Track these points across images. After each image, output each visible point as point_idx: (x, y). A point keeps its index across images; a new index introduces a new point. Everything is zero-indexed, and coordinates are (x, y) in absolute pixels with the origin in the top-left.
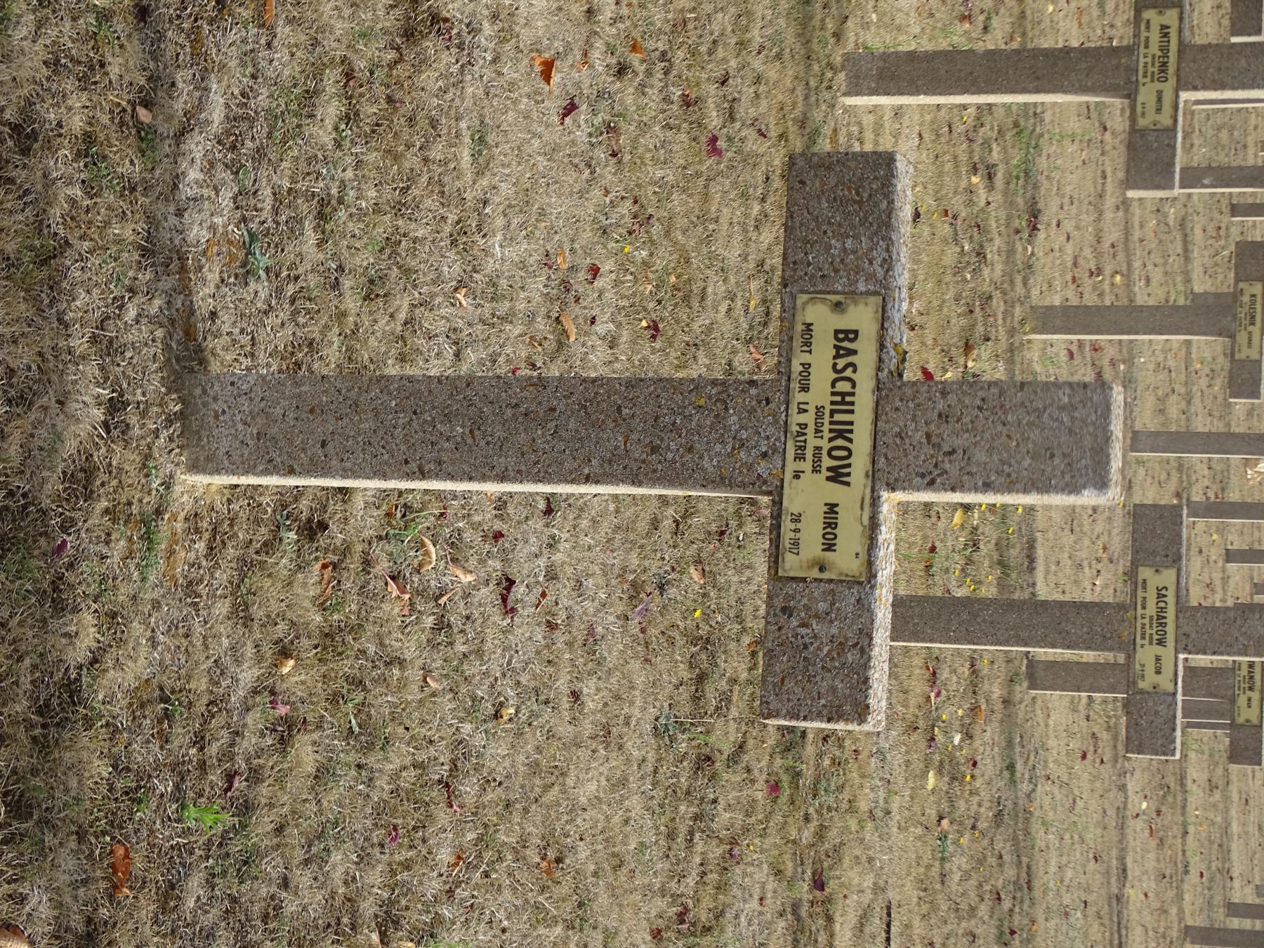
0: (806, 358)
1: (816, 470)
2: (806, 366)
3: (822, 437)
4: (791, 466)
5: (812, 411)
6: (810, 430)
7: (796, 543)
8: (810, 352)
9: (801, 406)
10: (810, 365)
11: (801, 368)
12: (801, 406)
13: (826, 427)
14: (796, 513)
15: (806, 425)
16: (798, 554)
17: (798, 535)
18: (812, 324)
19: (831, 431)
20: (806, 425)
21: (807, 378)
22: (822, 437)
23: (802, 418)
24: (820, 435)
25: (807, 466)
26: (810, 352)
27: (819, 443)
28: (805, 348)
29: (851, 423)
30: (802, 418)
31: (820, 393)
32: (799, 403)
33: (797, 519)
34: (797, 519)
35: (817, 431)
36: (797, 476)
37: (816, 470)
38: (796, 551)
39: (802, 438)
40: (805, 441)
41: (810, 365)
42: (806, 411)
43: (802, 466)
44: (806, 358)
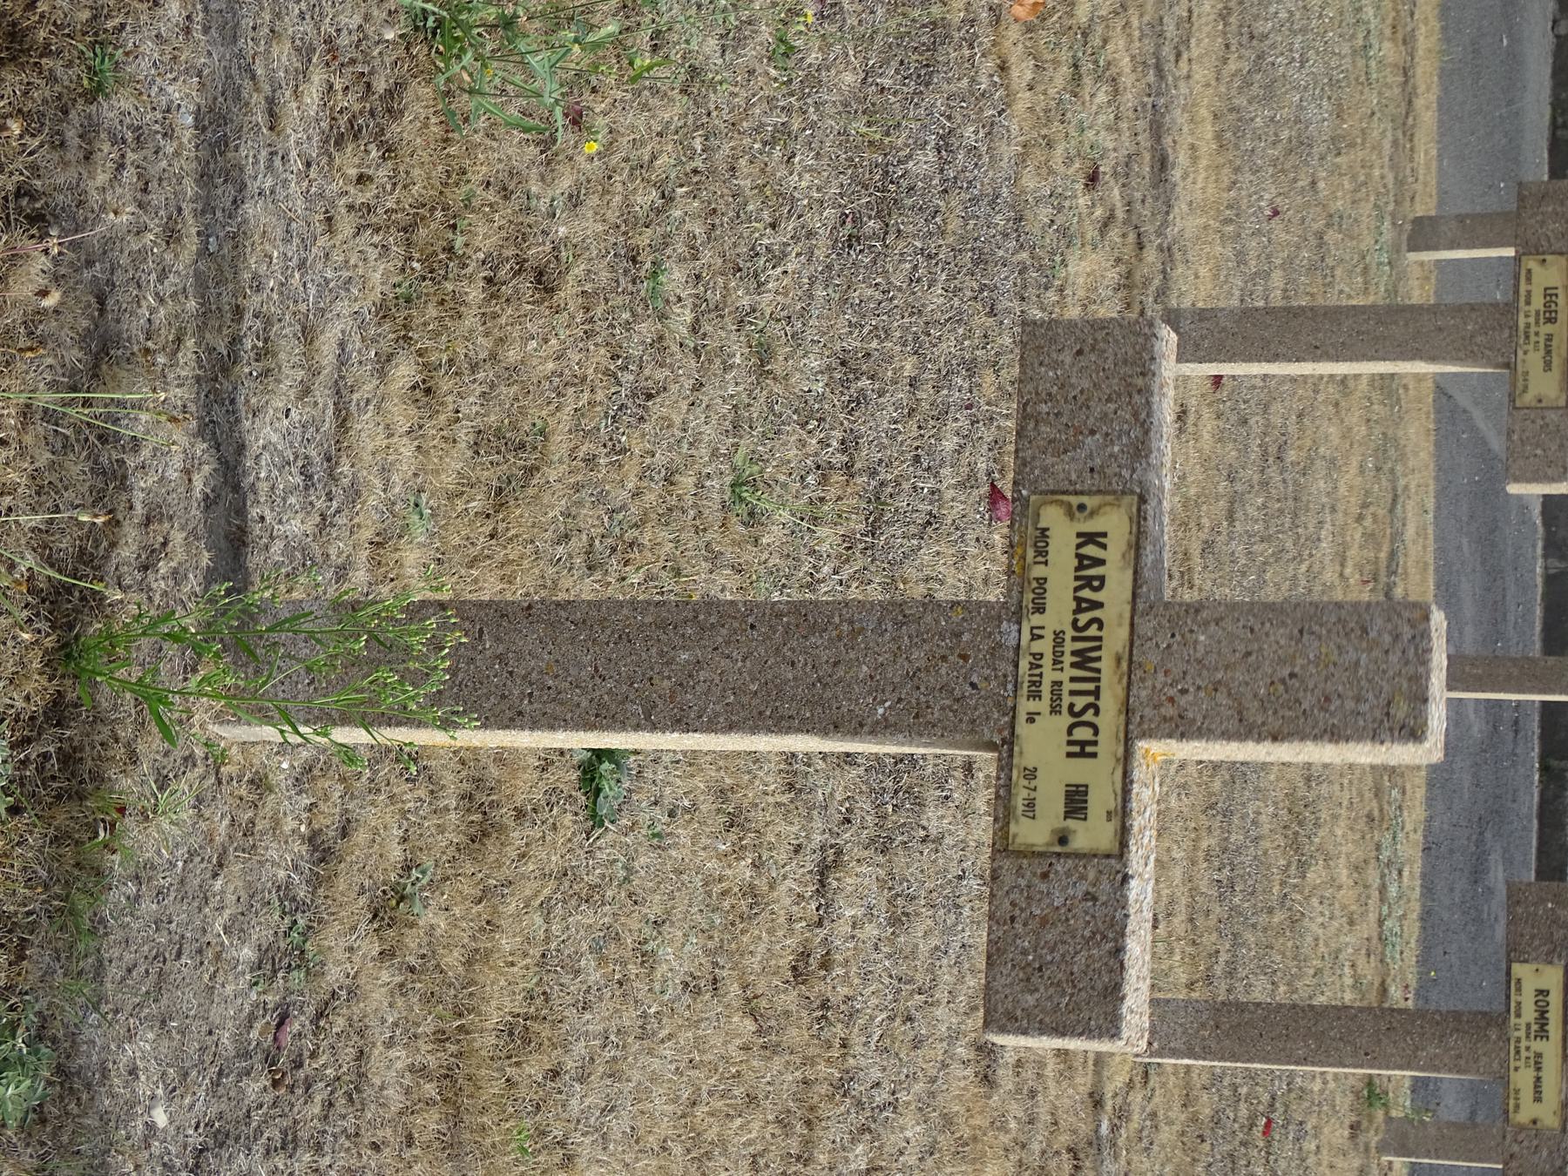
0: (1038, 571)
1: (1055, 710)
2: (1042, 581)
3: (1062, 669)
4: (1025, 706)
5: (1049, 637)
6: (1047, 661)
7: (1031, 805)
8: (1046, 563)
9: (1035, 631)
10: (1045, 579)
11: (1035, 584)
12: (1035, 631)
13: (1068, 659)
14: (1030, 767)
15: (1042, 655)
16: (1034, 818)
17: (1033, 795)
18: (1048, 529)
19: (1074, 653)
20: (1042, 655)
21: (1041, 596)
22: (1062, 669)
23: (1037, 647)
24: (1059, 666)
25: (1043, 705)
26: (1046, 563)
27: (1057, 676)
28: (1040, 559)
29: (1099, 639)
30: (1037, 647)
31: (1059, 612)
32: (1032, 628)
33: (1031, 774)
34: (1031, 774)
35: (1055, 662)
36: (1031, 720)
37: (1055, 710)
38: (1031, 814)
39: (1037, 671)
40: (1041, 675)
41: (1045, 579)
42: (1041, 637)
43: (1032, 706)
44: (1038, 571)
